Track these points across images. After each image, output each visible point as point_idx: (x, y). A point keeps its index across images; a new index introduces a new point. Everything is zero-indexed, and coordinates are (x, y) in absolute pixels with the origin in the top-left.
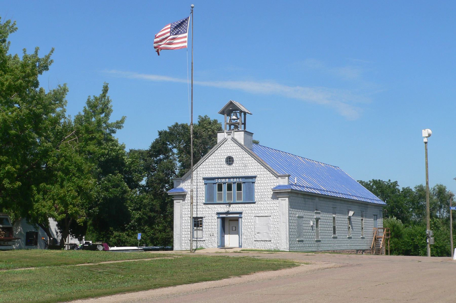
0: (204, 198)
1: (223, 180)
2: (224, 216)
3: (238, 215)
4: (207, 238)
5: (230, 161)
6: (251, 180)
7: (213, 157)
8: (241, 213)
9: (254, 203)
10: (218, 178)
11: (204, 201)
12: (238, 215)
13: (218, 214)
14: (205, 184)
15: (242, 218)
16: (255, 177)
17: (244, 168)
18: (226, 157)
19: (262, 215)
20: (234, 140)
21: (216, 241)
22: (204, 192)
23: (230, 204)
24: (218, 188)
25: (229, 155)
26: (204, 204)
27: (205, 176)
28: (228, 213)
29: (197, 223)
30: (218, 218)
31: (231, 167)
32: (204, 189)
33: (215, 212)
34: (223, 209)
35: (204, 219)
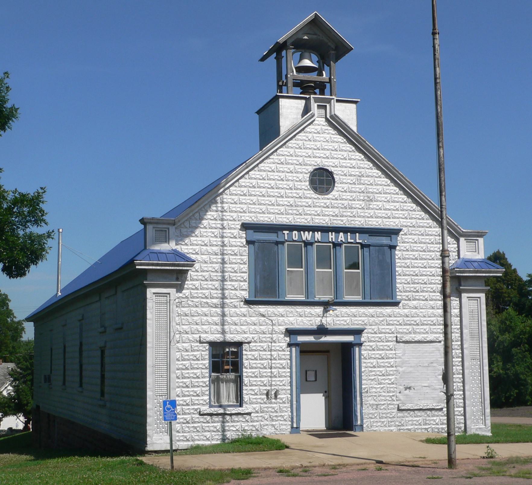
0: (245, 285)
1: (307, 236)
2: (310, 339)
3: (349, 338)
4: (257, 406)
5: (322, 180)
6: (385, 240)
7: (273, 166)
8: (358, 332)
9: (396, 304)
10: (291, 228)
11: (245, 294)
12: (349, 338)
13: (290, 332)
14: (249, 242)
15: (360, 345)
16: (394, 232)
17: (363, 204)
18: (311, 169)
19: (418, 337)
20: (336, 124)
21: (287, 414)
22: (245, 268)
23: (326, 305)
24: (273, 255)
25: (328, 164)
26: (248, 302)
27: (248, 218)
28: (322, 331)
29: (226, 359)
30: (290, 345)
31: (323, 200)
32: (246, 258)
33: (283, 328)
34: (308, 318)
35: (245, 346)
